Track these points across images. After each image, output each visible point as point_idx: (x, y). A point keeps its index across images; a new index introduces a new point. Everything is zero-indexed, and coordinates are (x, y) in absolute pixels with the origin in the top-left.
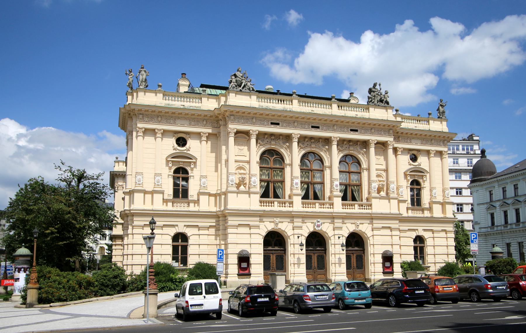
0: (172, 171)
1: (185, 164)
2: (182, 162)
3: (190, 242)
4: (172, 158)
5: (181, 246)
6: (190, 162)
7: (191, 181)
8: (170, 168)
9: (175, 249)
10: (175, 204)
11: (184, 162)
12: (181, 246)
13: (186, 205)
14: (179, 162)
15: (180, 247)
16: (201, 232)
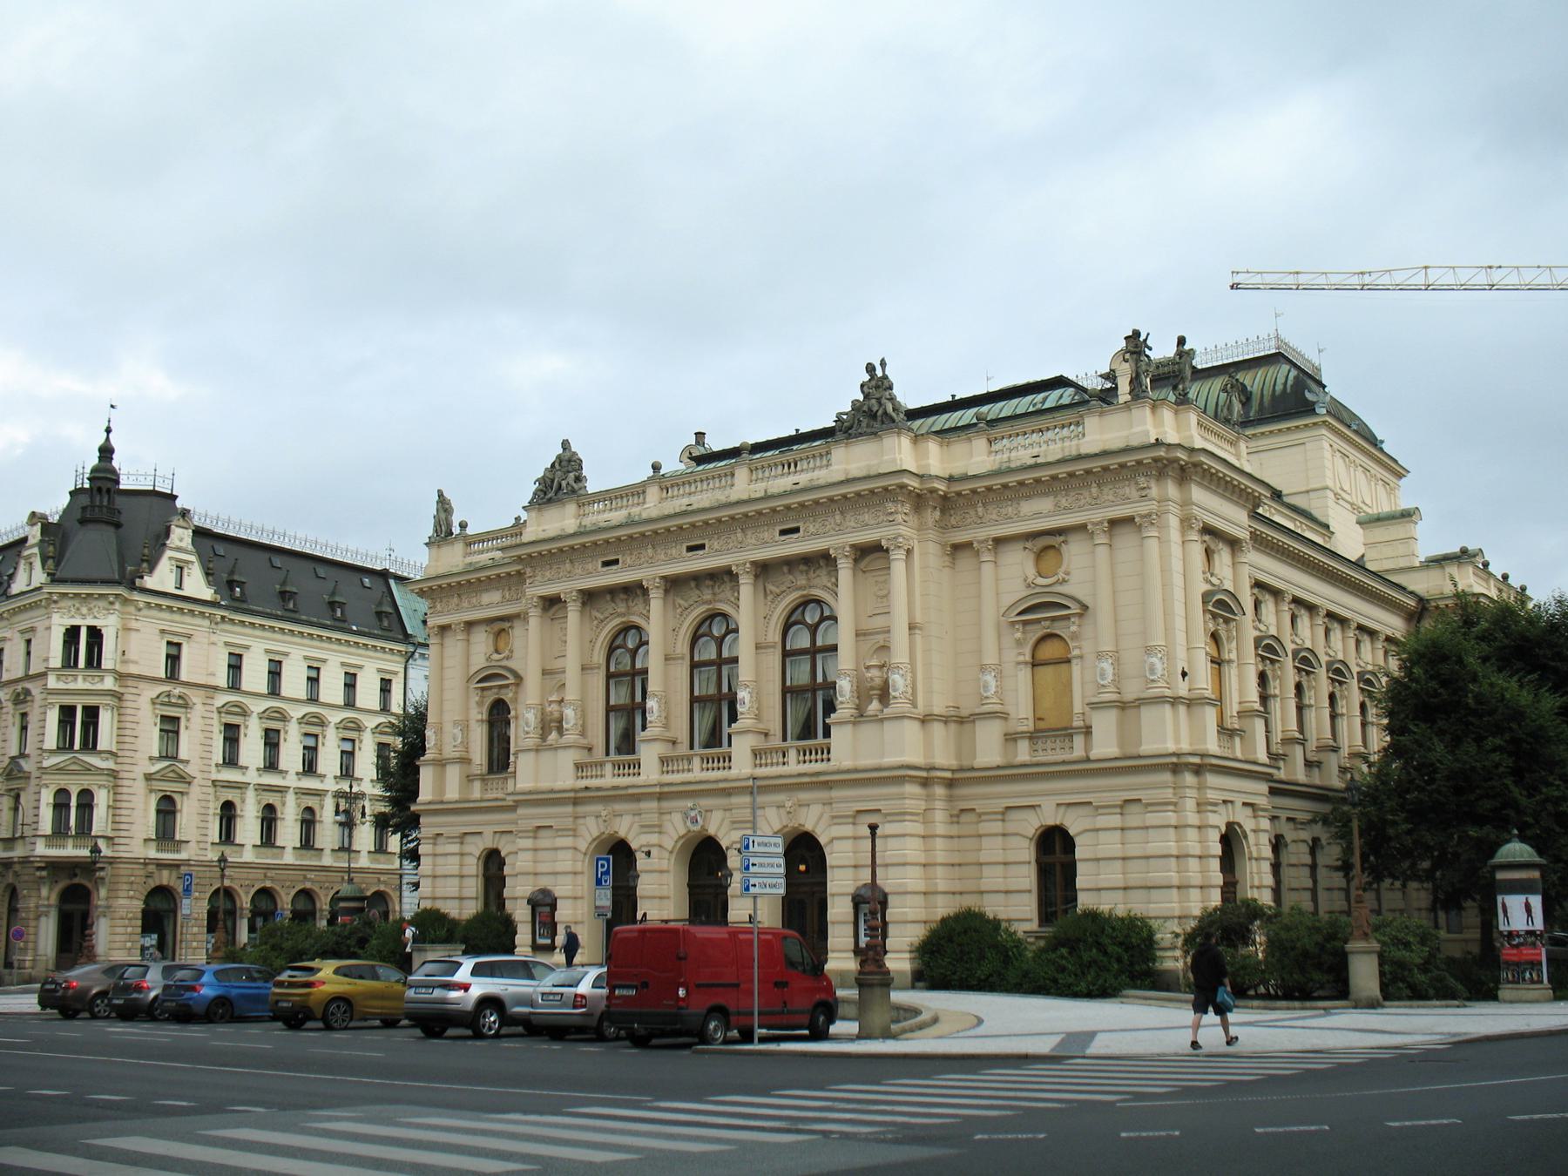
0: (1028, 650)
1: (1057, 624)
2: (1046, 619)
3: (1079, 853)
4: (1020, 614)
5: (1062, 865)
6: (1067, 617)
7: (1076, 668)
8: (1019, 643)
9: (1044, 872)
10: (1040, 745)
11: (1053, 619)
12: (1062, 865)
13: (1067, 744)
14: (1038, 621)
15: (1058, 868)
16: (1102, 821)
